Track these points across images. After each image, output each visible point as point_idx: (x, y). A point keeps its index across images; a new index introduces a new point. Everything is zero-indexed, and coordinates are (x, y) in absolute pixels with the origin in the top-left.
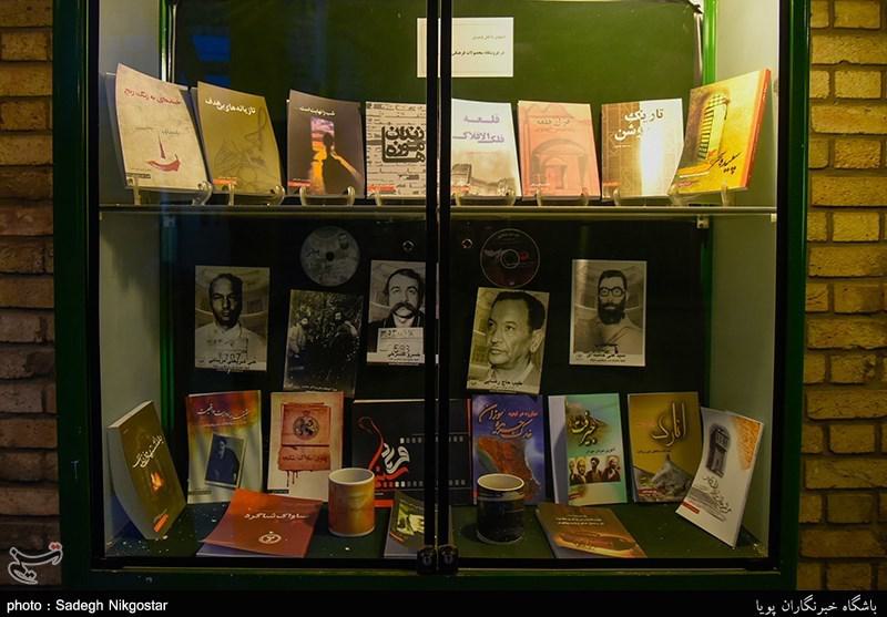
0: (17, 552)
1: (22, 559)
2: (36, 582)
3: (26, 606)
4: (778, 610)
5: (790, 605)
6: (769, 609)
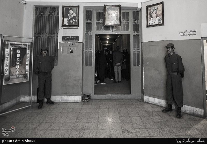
0: (4, 129)
1: (5, 130)
2: (9, 136)
4: (182, 142)
5: (184, 140)
6: (180, 141)
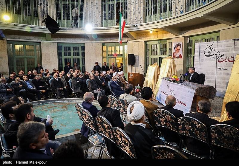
2: (10, 157)
3: (8, 163)
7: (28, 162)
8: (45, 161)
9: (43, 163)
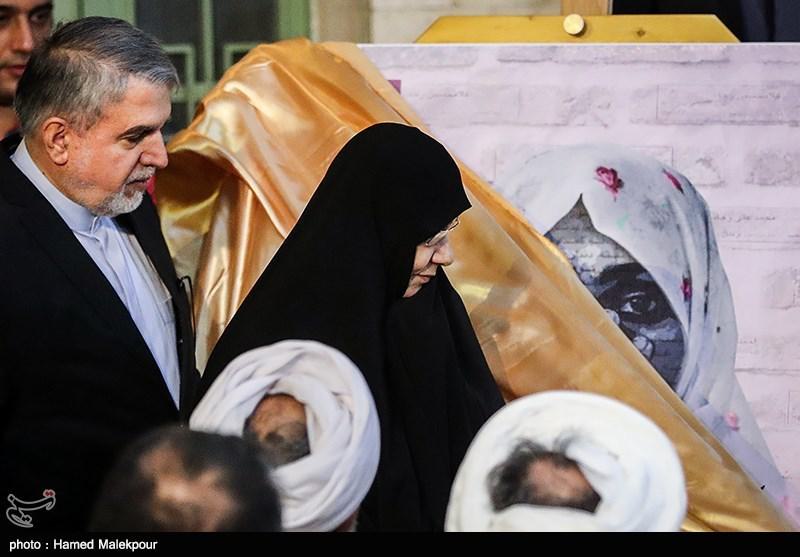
1: (19, 505)
2: (32, 526)
3: (27, 545)
7: (92, 542)
8: (149, 541)
9: (142, 545)
